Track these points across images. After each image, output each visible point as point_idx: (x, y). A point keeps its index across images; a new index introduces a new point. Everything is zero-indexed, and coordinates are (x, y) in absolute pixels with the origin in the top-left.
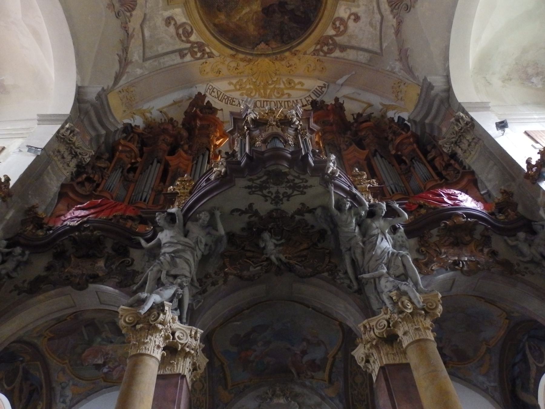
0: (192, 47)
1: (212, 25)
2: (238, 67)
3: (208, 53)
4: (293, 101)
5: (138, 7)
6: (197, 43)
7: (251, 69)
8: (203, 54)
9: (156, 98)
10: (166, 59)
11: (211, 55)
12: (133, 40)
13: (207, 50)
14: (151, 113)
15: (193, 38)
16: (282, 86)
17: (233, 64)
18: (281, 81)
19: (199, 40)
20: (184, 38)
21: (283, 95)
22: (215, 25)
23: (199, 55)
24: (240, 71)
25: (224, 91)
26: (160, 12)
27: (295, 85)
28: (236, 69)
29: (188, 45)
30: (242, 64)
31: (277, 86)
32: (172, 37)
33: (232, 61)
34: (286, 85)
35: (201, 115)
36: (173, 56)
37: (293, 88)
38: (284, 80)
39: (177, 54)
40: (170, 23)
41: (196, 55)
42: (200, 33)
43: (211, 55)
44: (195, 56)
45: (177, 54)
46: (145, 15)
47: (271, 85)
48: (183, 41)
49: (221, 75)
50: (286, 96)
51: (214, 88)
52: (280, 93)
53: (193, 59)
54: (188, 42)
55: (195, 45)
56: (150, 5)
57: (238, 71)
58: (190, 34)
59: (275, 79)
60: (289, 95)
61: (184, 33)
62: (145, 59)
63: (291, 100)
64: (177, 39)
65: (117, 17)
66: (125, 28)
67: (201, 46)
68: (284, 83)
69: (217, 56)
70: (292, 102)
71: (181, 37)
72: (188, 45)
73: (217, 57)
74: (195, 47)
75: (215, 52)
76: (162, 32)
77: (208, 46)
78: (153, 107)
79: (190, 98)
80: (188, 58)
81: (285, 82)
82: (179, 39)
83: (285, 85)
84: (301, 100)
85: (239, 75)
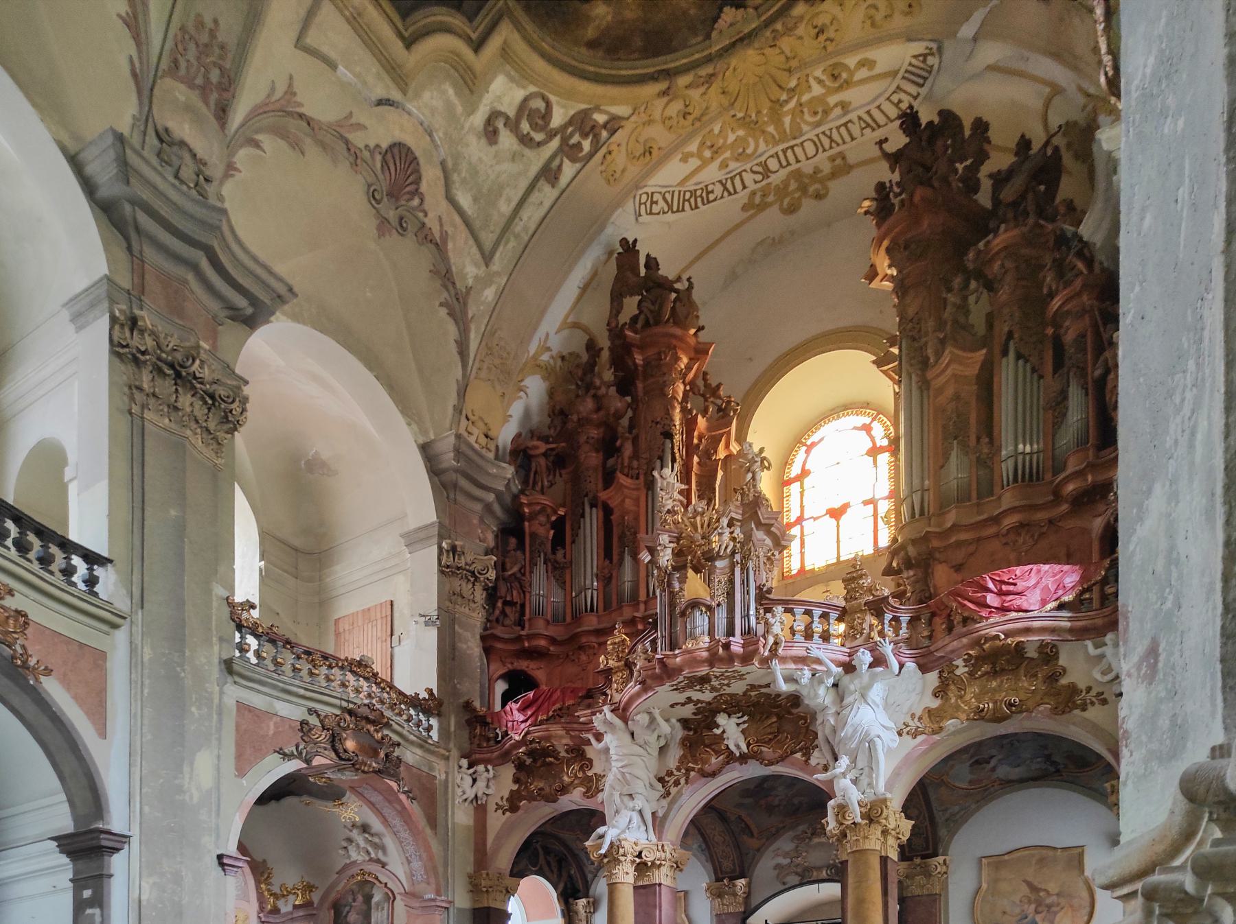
0: (564, 141)
1: (583, 50)
2: (690, 109)
3: (605, 126)
4: (860, 118)
5: (422, 161)
6: (570, 122)
7: (724, 93)
8: (596, 137)
9: (543, 312)
10: (525, 218)
11: (613, 125)
12: (450, 245)
13: (600, 118)
14: (549, 349)
15: (557, 119)
16: (817, 90)
17: (676, 107)
18: (811, 80)
19: (572, 112)
20: (538, 137)
21: (826, 112)
22: (592, 45)
23: (587, 145)
24: (697, 113)
25: (678, 185)
26: (467, 126)
27: (851, 73)
28: (685, 115)
29: (555, 143)
30: (695, 94)
31: (805, 98)
32: (514, 157)
33: (667, 104)
34: (828, 83)
35: (638, 336)
36: (535, 197)
37: (848, 84)
38: (818, 73)
39: (542, 182)
40: (495, 132)
41: (581, 149)
42: (569, 95)
43: (613, 125)
44: (580, 155)
45: (542, 182)
46: (443, 164)
47: (786, 102)
48: (539, 144)
49: (655, 152)
50: (838, 111)
51: (652, 193)
52: (820, 110)
53: (578, 165)
54: (551, 135)
55: (570, 129)
56: (441, 135)
57: (690, 118)
58: (547, 115)
59: (793, 84)
60: (844, 106)
61: (534, 127)
62: (487, 259)
63: (853, 116)
64: (527, 152)
65: (402, 235)
66: (425, 236)
67: (582, 123)
68: (820, 82)
69: (626, 115)
70: (856, 120)
71: (531, 139)
72: (555, 143)
73: (628, 118)
74: (572, 135)
75: (621, 110)
76: (492, 166)
77: (597, 109)
78: (547, 335)
79: (611, 253)
80: (569, 169)
81: (824, 77)
82: (531, 148)
83: (824, 86)
84: (879, 107)
85: (698, 124)
